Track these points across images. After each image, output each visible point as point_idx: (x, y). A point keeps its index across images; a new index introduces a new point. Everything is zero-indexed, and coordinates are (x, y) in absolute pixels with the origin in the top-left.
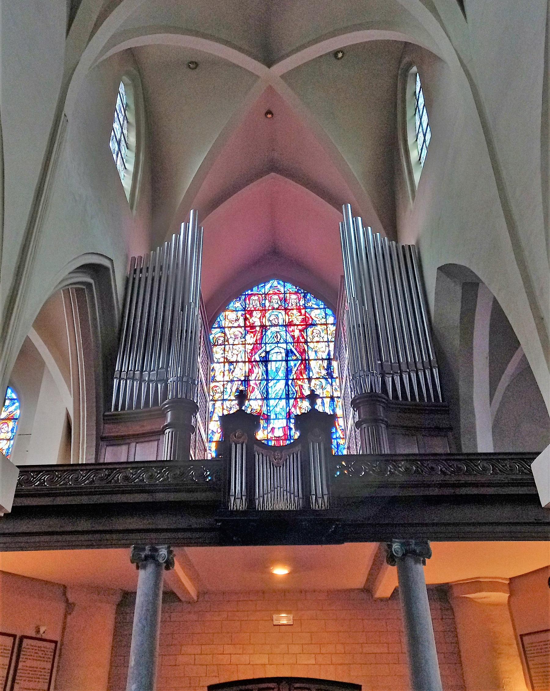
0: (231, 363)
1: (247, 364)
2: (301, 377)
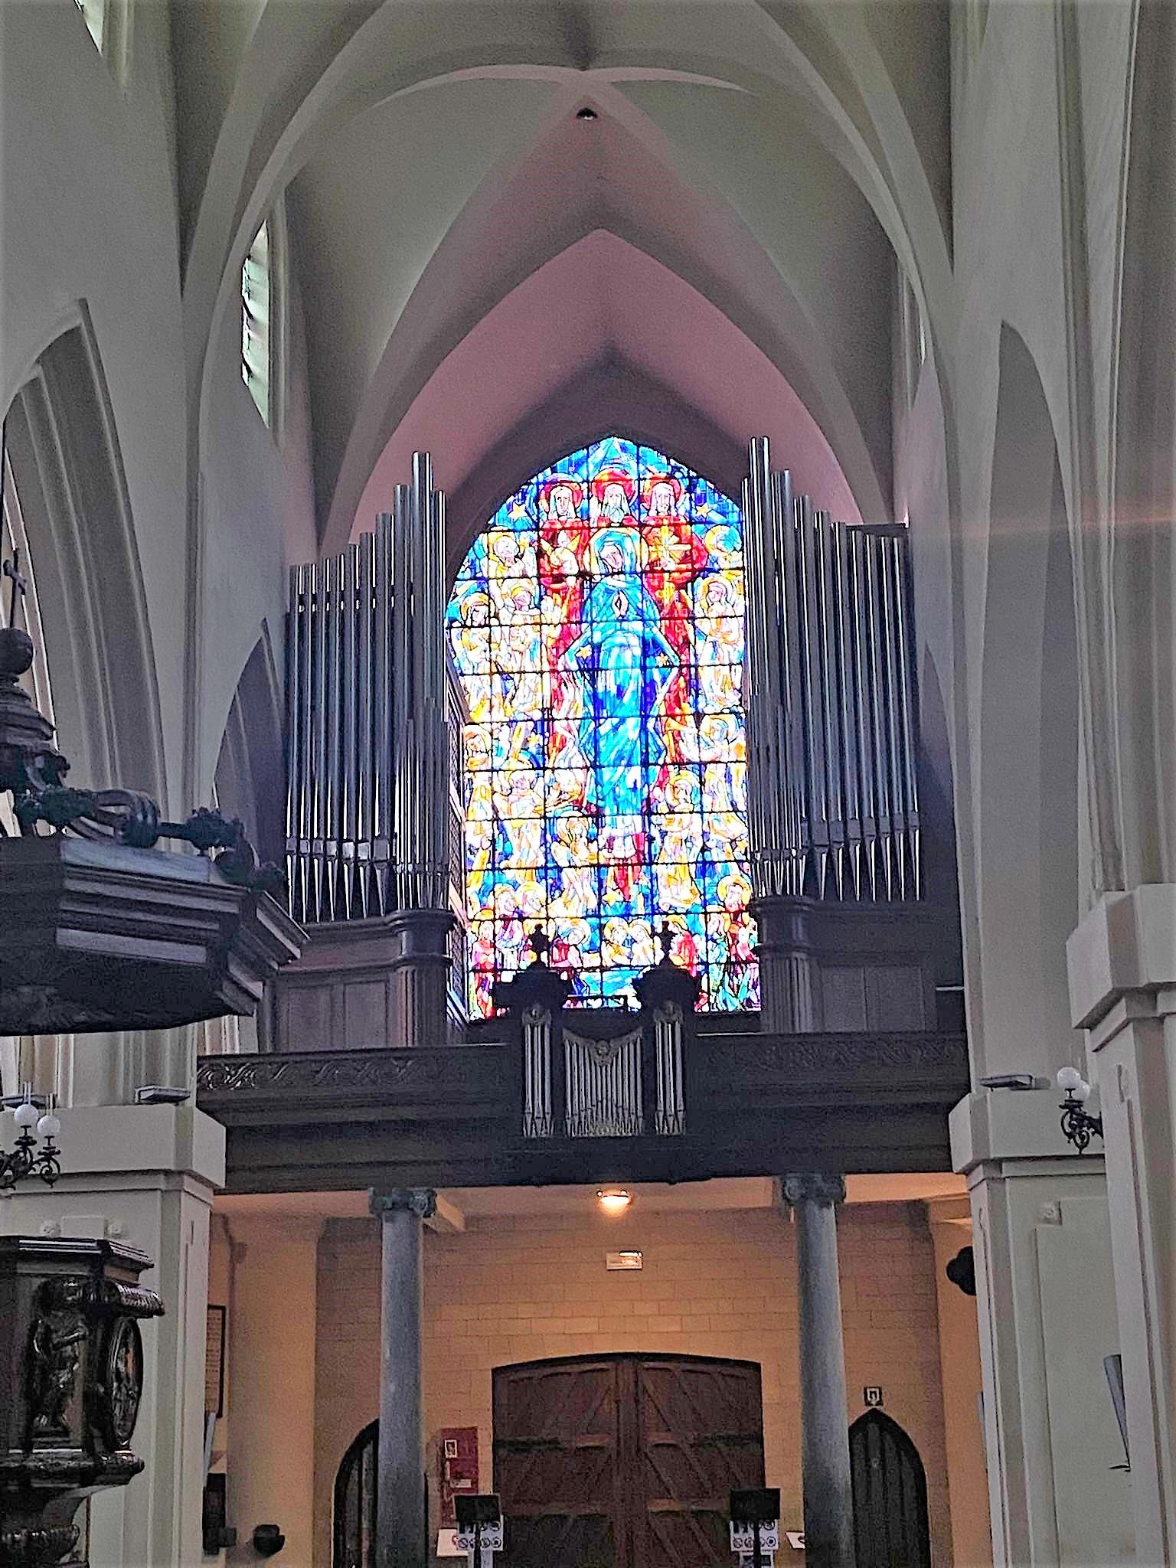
0: (505, 675)
1: (546, 676)
2: (677, 711)
